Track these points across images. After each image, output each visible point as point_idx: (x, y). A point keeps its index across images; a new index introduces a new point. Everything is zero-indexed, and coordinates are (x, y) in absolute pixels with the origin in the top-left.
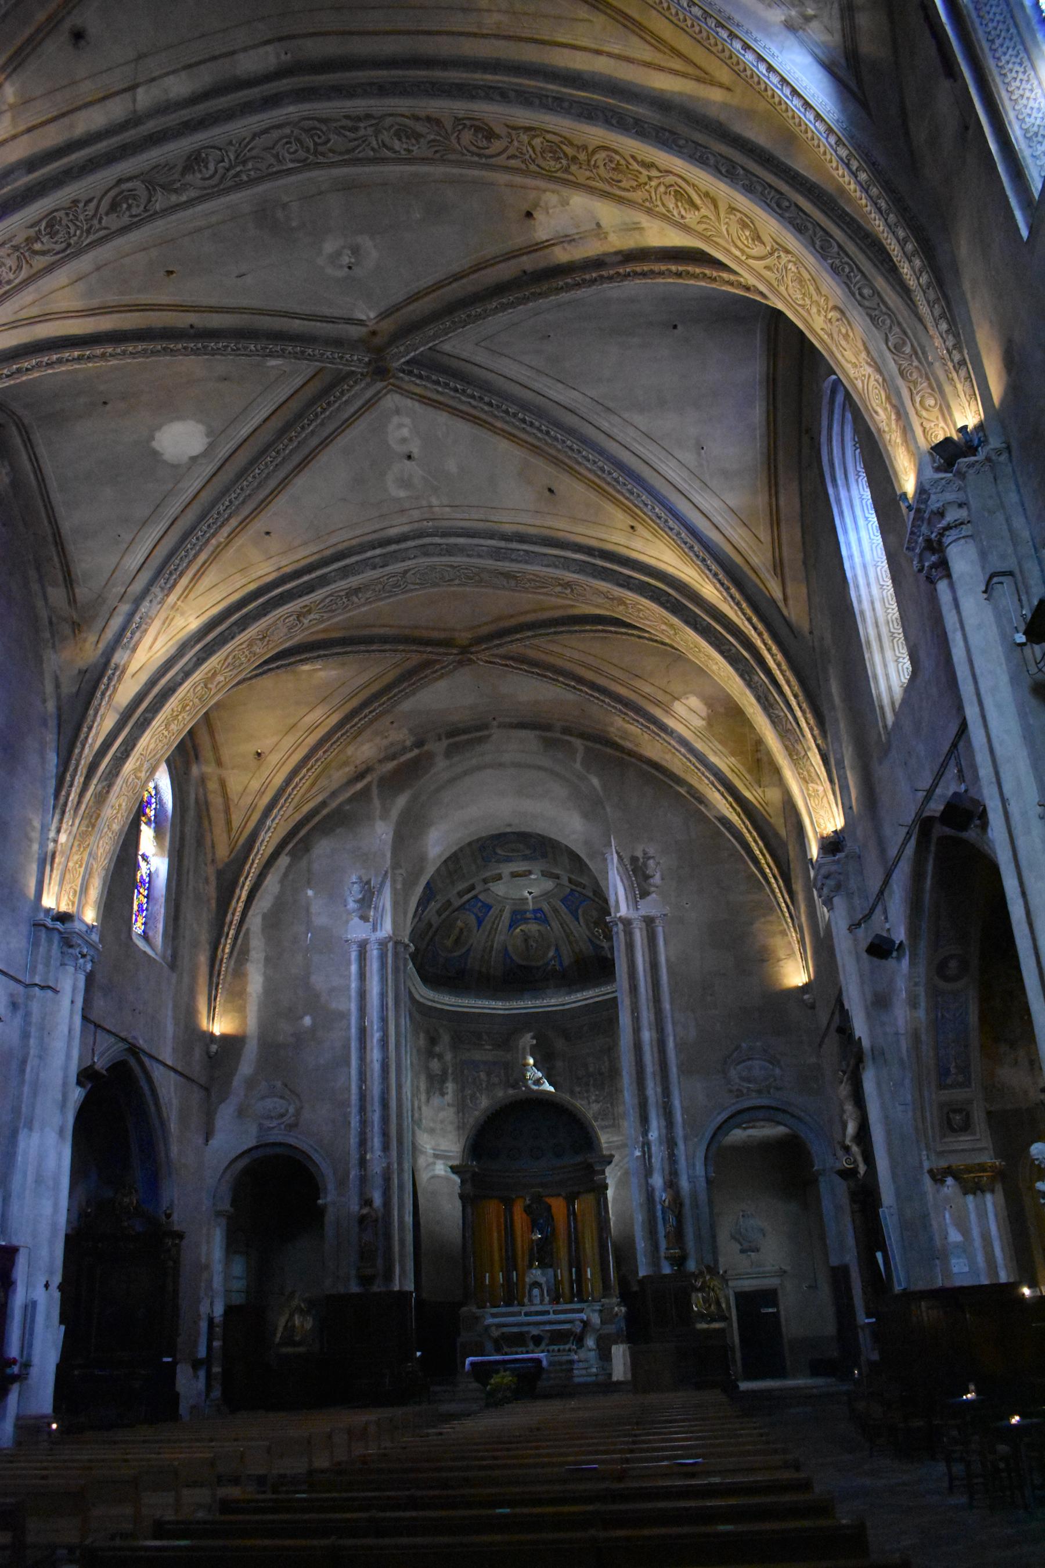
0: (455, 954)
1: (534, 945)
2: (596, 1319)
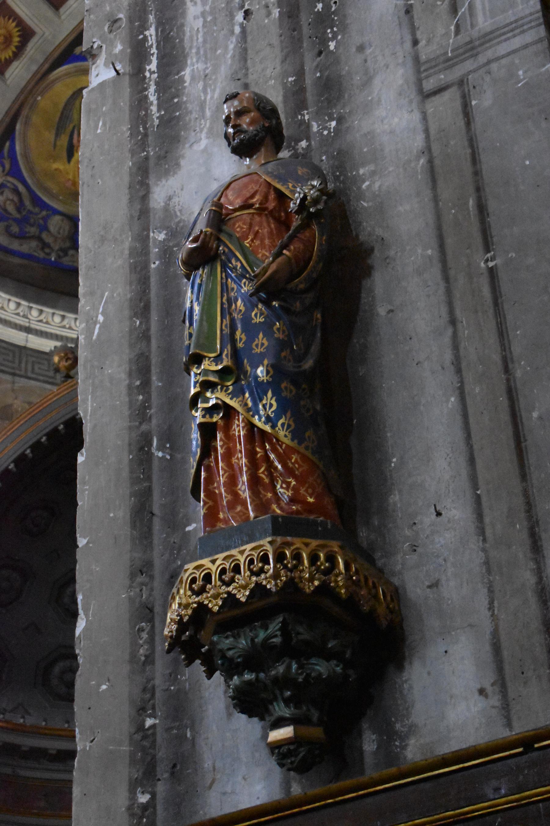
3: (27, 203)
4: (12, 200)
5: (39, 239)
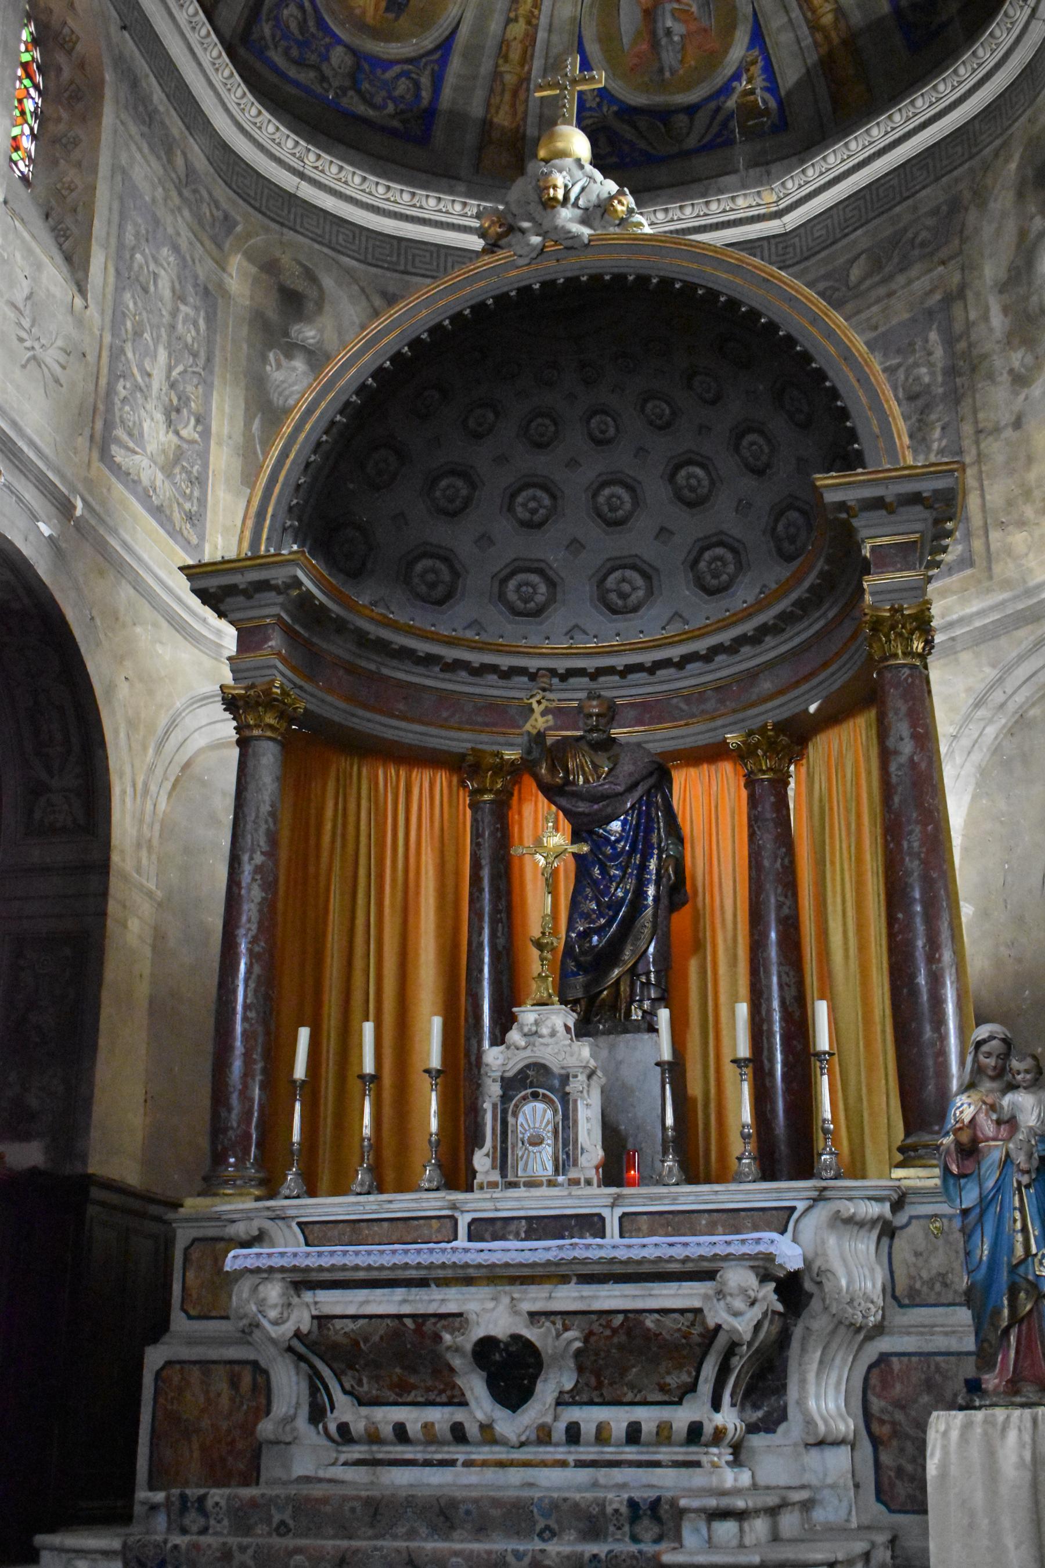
0: (394, 50)
1: (679, 29)
2: (856, 1271)
3: (311, 23)
4: (296, 18)
5: (317, 68)
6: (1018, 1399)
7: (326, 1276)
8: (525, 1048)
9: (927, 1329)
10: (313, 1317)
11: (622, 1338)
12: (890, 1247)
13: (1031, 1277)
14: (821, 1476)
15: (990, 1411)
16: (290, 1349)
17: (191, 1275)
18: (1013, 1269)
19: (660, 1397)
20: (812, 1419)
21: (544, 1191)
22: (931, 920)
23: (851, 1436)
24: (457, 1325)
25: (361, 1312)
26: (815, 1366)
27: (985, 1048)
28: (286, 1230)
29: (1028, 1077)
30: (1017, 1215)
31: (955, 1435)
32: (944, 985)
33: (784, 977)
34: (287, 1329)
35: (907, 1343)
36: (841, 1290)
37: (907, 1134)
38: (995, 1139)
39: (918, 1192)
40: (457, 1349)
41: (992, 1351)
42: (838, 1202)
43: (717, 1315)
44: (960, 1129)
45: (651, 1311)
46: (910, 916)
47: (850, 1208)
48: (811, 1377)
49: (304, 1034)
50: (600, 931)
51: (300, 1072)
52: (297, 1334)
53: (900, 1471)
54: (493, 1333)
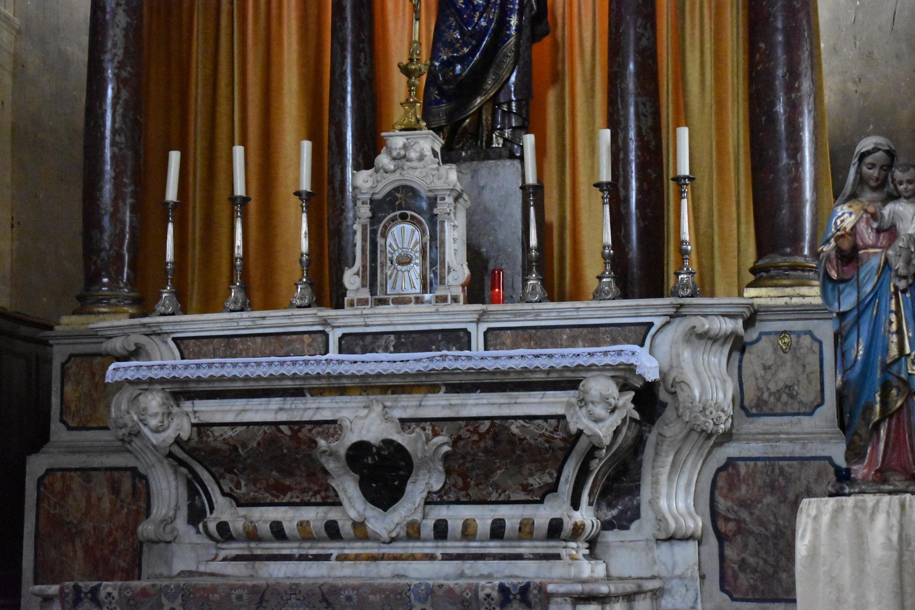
2: (708, 383)
6: (887, 487)
7: (203, 387)
8: (394, 171)
9: (772, 437)
10: (193, 425)
11: (490, 443)
12: (741, 361)
13: (903, 376)
14: (670, 569)
15: (860, 497)
16: (170, 455)
17: (68, 388)
18: (886, 368)
19: (522, 496)
20: (664, 517)
21: (412, 307)
22: (792, 47)
23: (699, 533)
24: (331, 431)
25: (238, 420)
26: (667, 469)
27: (869, 160)
28: (163, 347)
29: (910, 187)
30: (893, 317)
31: (825, 519)
32: (801, 114)
33: (641, 107)
34: (169, 435)
35: (755, 449)
36: (694, 399)
37: (760, 254)
38: (873, 247)
39: (768, 310)
40: (332, 454)
41: (862, 444)
42: (693, 318)
43: (579, 421)
44: (842, 236)
45: (516, 418)
46: (771, 47)
47: (704, 324)
48: (664, 478)
49: (175, 157)
50: (463, 60)
51: (172, 195)
52: (178, 441)
53: (743, 564)
54: (365, 439)
